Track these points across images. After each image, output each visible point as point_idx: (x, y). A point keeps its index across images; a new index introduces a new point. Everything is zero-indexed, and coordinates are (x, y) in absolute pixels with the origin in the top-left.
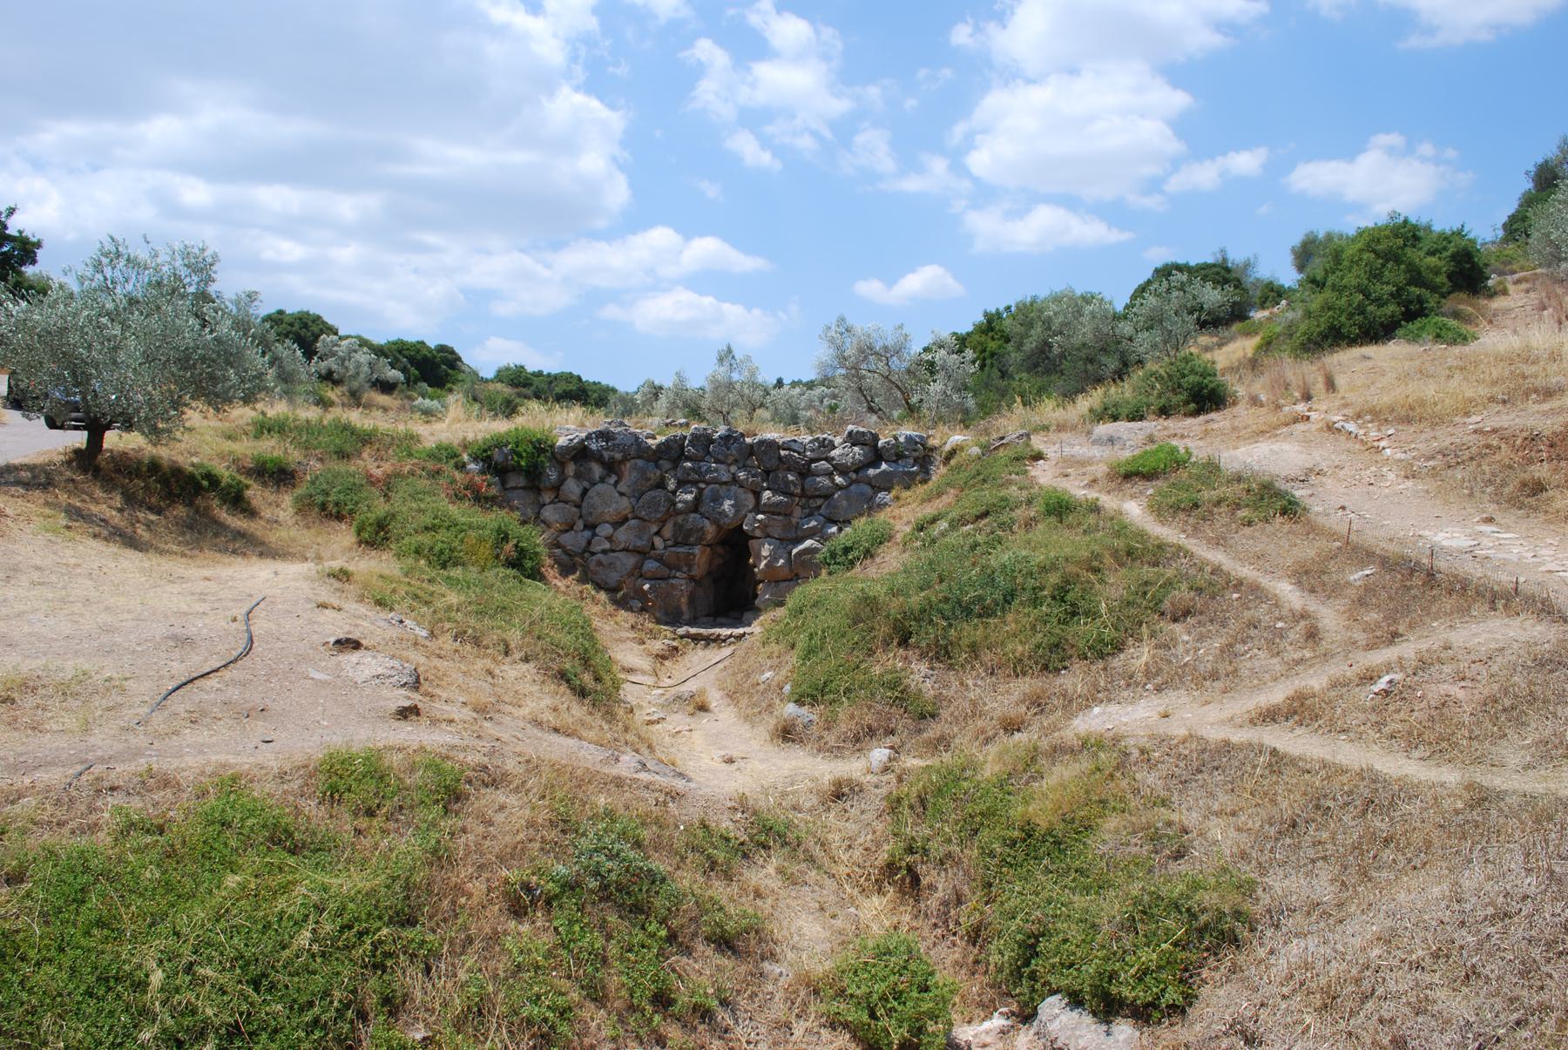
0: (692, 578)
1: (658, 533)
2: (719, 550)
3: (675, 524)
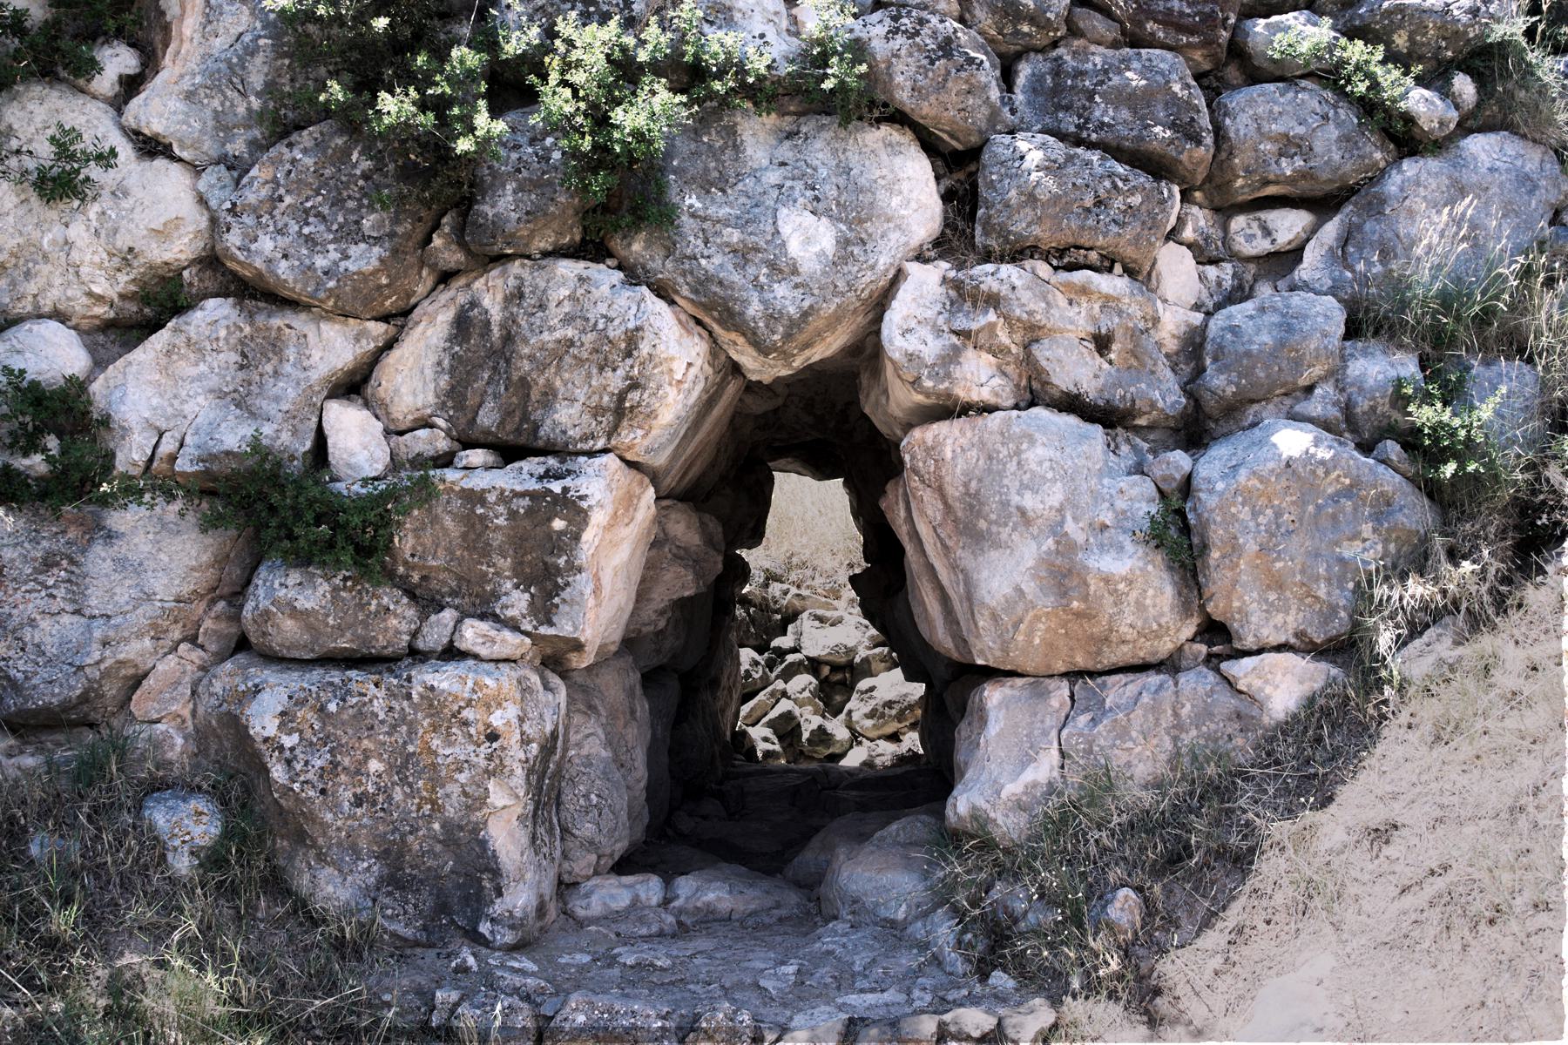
0: (553, 658)
1: (354, 385)
2: (684, 528)
3: (464, 325)
